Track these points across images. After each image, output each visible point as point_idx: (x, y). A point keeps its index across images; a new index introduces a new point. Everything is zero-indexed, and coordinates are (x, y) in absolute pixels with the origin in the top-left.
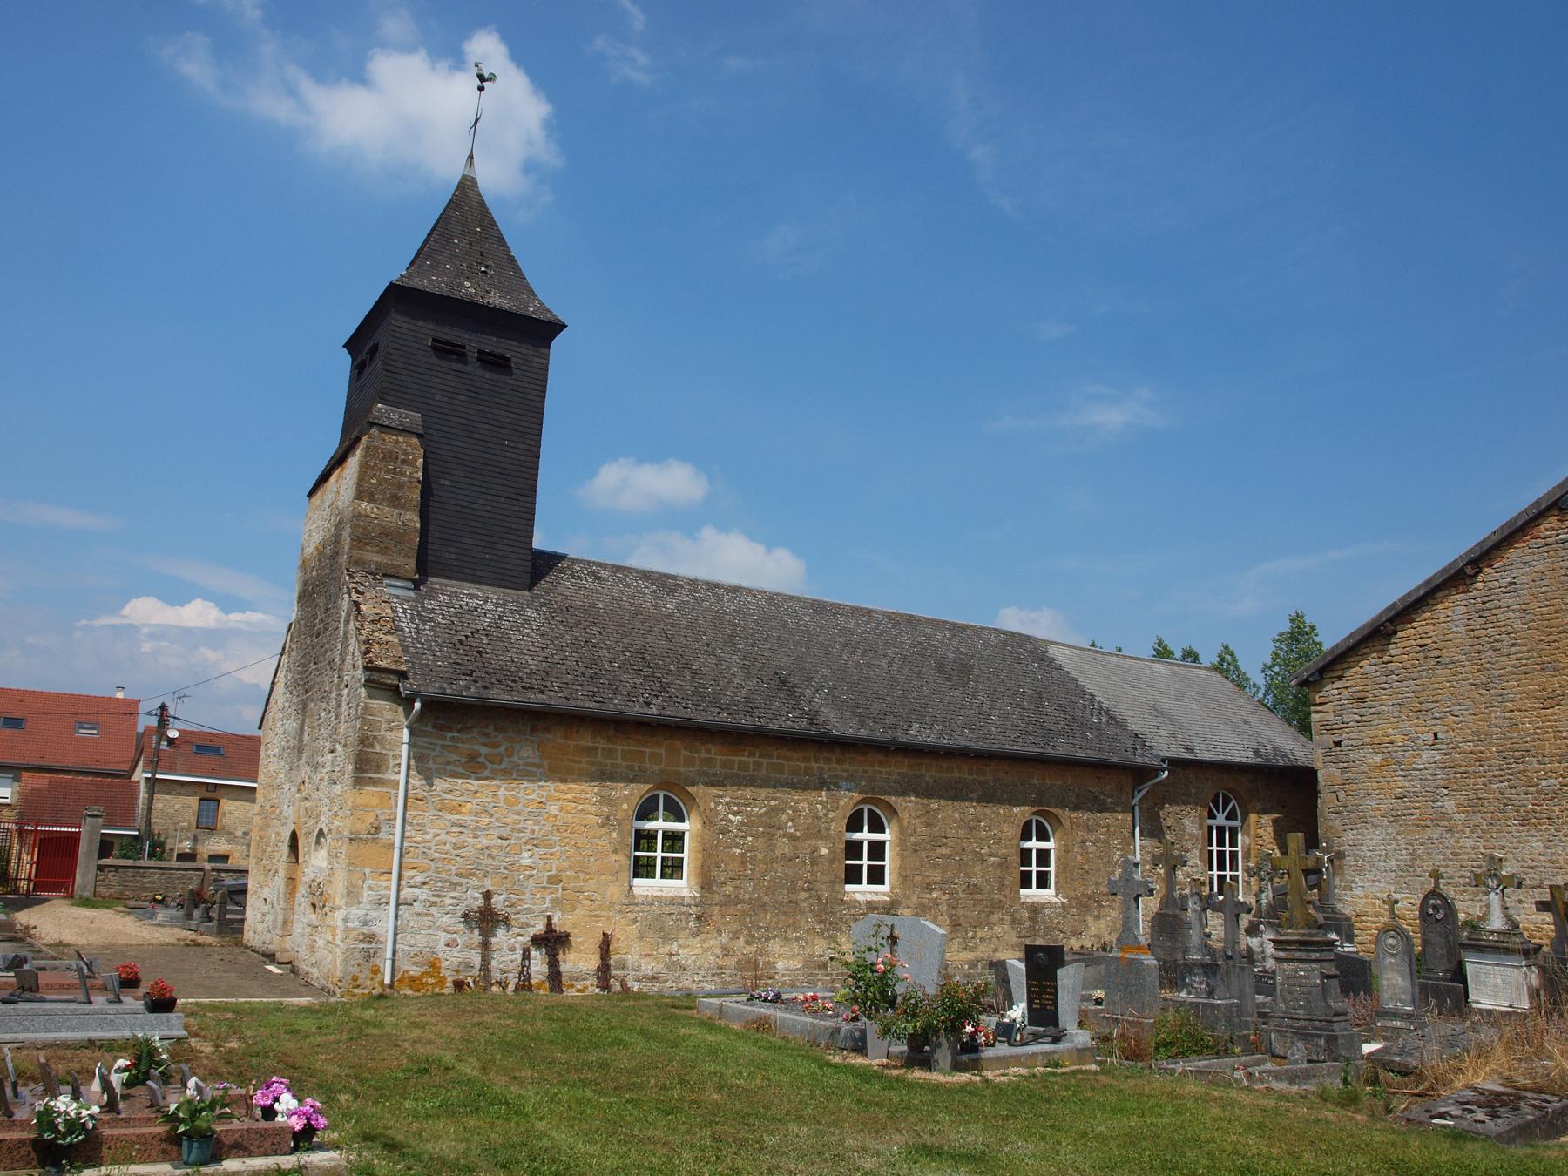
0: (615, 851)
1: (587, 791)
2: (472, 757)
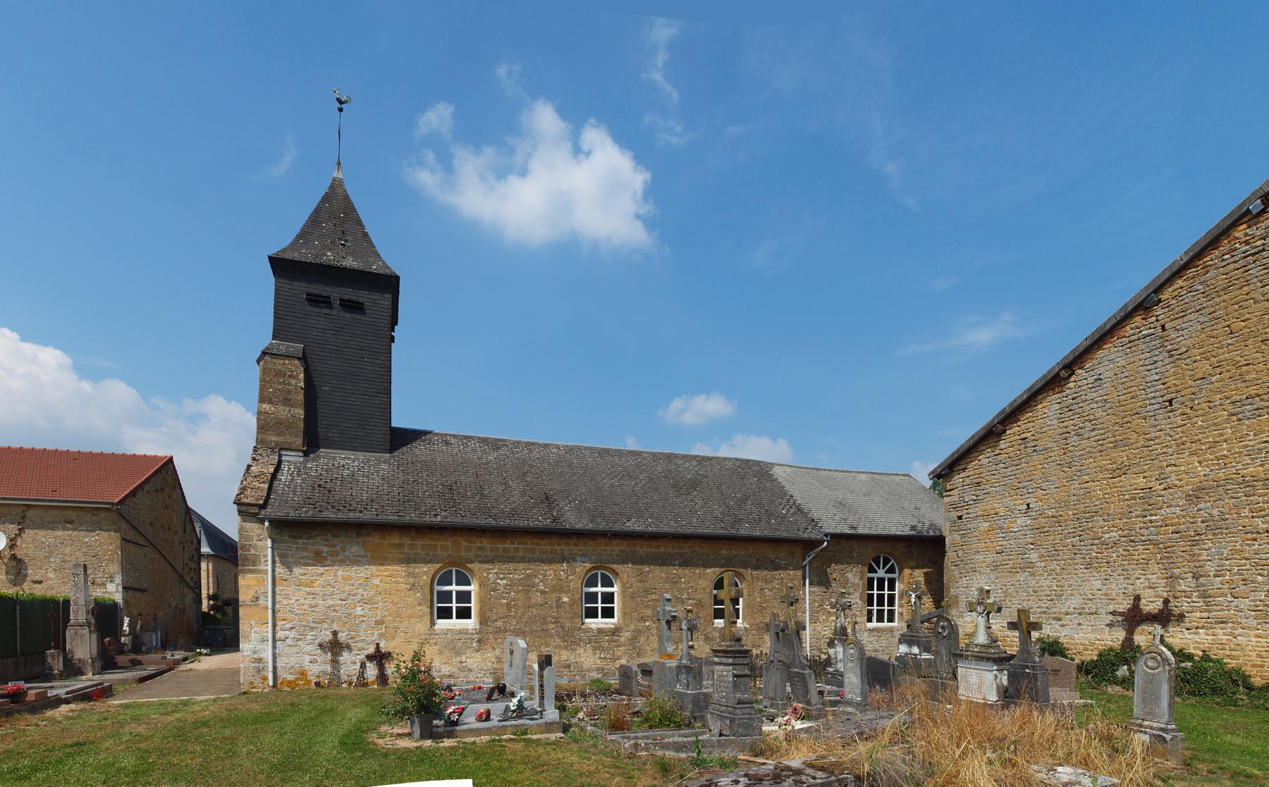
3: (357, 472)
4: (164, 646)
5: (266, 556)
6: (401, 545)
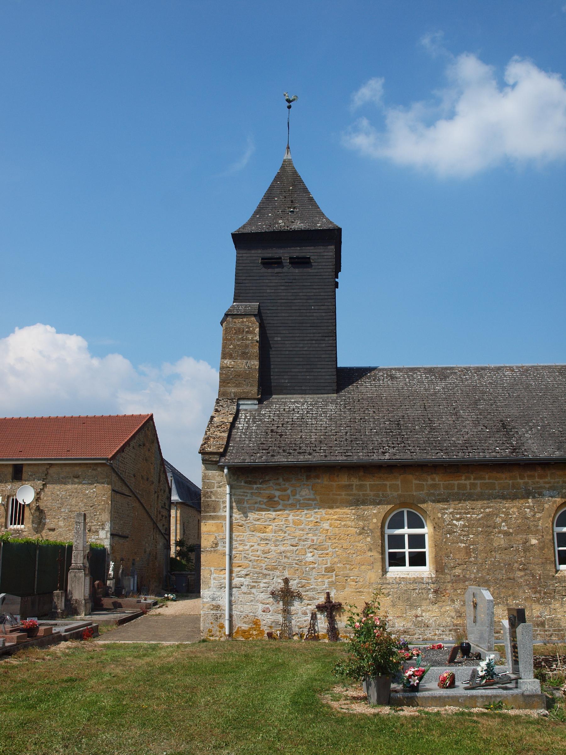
0: (370, 550)
1: (347, 513)
2: (271, 498)
3: (308, 415)
4: (141, 590)
5: (224, 502)
6: (349, 487)
